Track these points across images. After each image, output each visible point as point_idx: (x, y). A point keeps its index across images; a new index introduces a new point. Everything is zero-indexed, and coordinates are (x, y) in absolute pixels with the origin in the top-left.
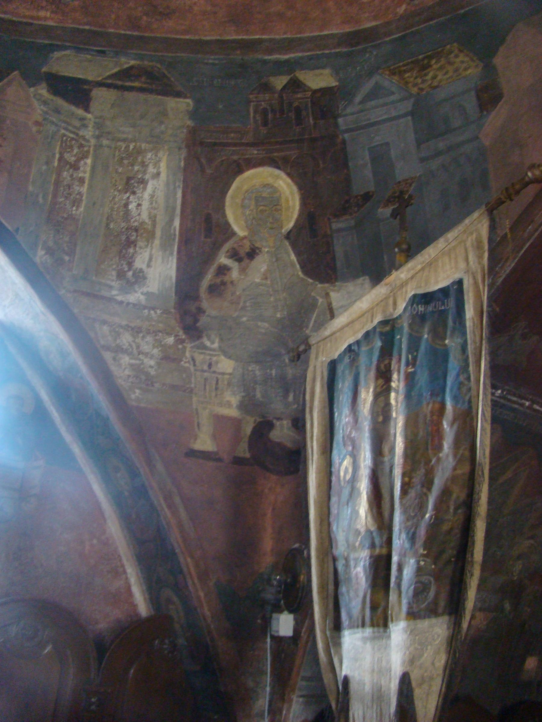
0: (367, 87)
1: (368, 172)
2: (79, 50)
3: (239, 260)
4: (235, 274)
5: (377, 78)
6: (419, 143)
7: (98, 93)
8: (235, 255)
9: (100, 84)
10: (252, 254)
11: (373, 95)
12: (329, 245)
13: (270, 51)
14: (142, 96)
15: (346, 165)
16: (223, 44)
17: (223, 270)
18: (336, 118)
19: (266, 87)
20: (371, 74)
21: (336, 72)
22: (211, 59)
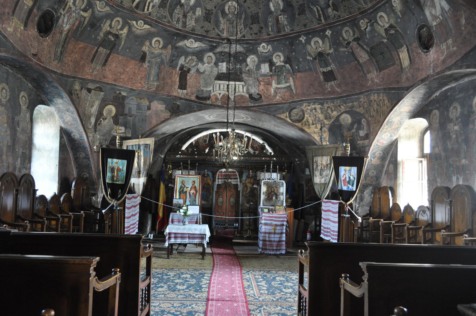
0: (131, 98)
1: (127, 111)
2: (92, 83)
3: (103, 120)
4: (102, 122)
5: (133, 97)
6: (137, 110)
7: (93, 91)
8: (103, 119)
9: (93, 89)
10: (106, 119)
11: (130, 99)
12: (118, 120)
13: (118, 87)
14: (98, 92)
15: (124, 108)
16: (112, 84)
17: (101, 121)
18: (125, 100)
19: (115, 92)
20: (132, 96)
21: (127, 94)
22: (109, 86)
